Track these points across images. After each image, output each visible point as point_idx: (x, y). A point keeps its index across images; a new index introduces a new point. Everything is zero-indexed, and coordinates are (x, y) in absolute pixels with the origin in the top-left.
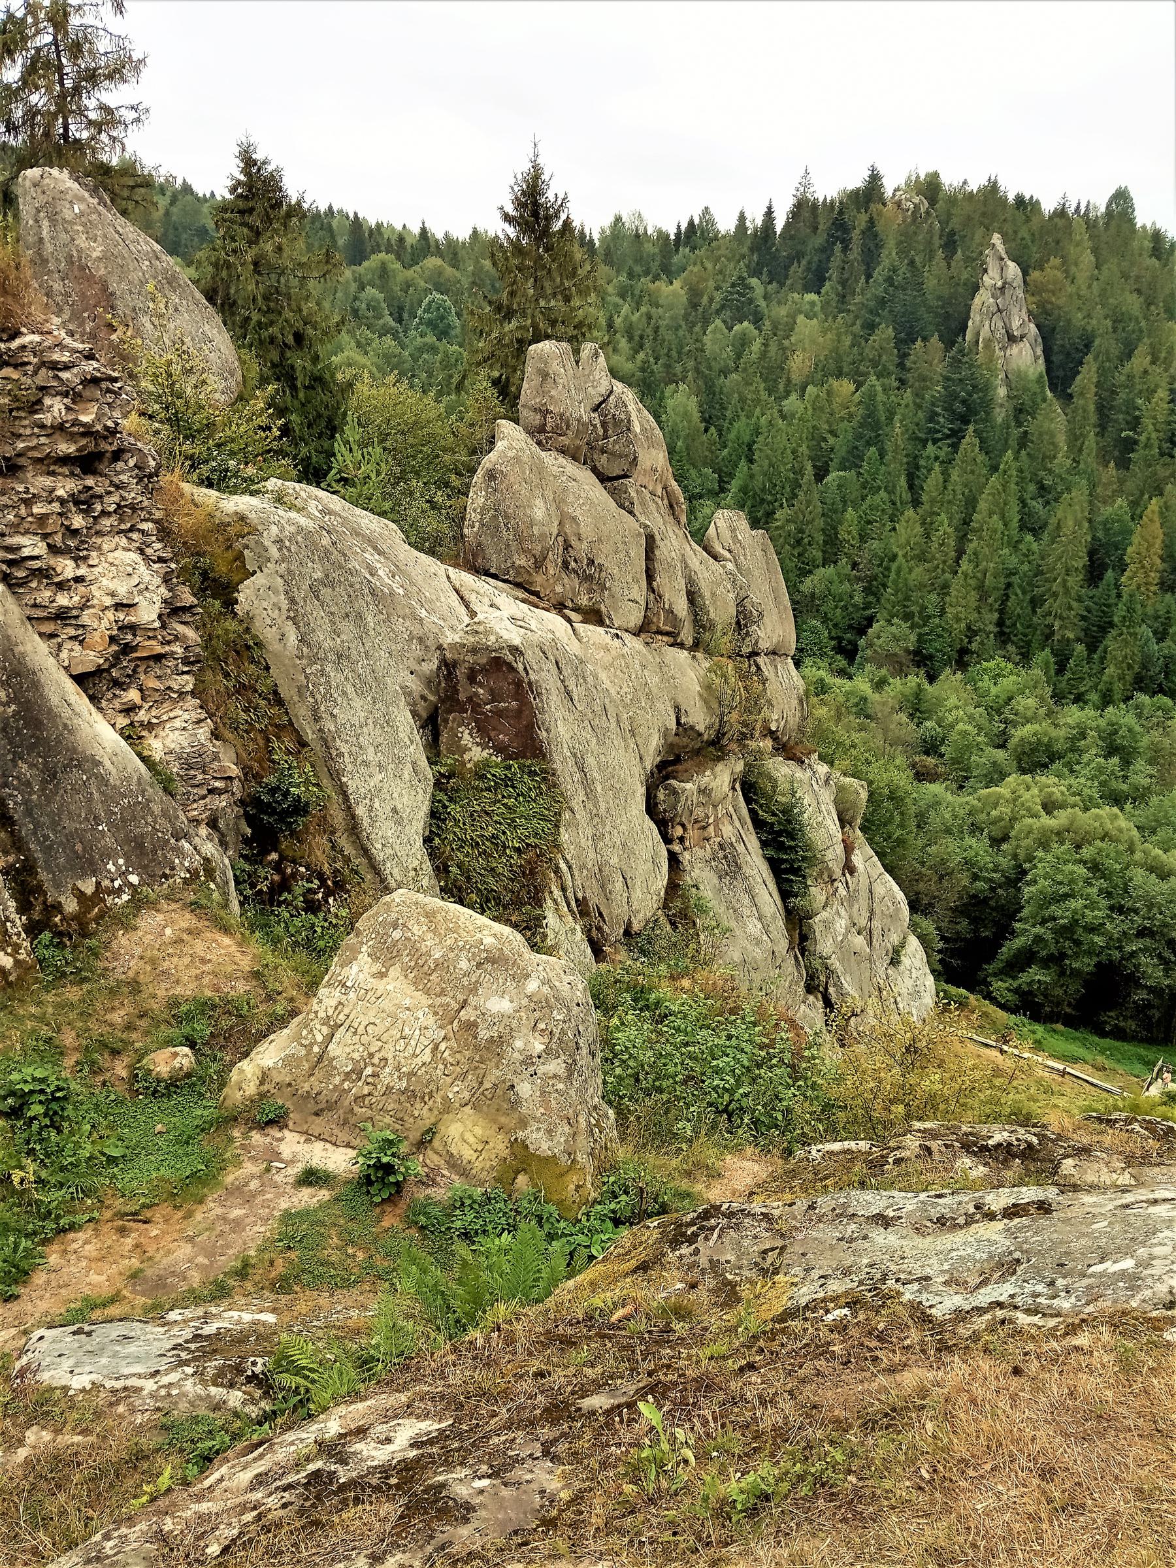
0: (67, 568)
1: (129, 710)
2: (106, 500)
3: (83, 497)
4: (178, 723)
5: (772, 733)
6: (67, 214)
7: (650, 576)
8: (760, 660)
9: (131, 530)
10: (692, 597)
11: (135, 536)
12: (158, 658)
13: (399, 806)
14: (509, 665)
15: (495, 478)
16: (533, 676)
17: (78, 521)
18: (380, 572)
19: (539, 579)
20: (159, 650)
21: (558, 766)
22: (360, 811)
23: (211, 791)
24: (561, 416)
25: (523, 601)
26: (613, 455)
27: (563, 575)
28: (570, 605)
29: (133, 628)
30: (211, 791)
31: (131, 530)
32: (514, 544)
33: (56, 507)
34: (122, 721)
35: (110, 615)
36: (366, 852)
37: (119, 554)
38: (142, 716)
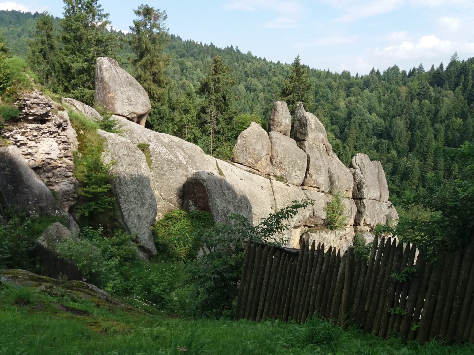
0: (33, 143)
1: (48, 178)
2: (45, 129)
3: (37, 129)
4: (64, 183)
5: (368, 225)
6: (103, 68)
7: (308, 169)
8: (364, 201)
9: (55, 137)
10: (330, 177)
11: (55, 138)
12: (60, 167)
13: (141, 214)
14: (202, 184)
15: (244, 137)
16: (209, 188)
17: (35, 134)
18: (180, 158)
19: (258, 166)
20: (60, 165)
21: (214, 214)
22: (125, 213)
23: (69, 200)
24: (279, 122)
25: (249, 171)
26: (302, 134)
27: (271, 166)
28: (273, 174)
29: (51, 159)
30: (69, 200)
31: (55, 137)
32: (248, 155)
33: (29, 130)
34: (46, 180)
35: (43, 155)
36: (126, 224)
37: (50, 142)
38: (52, 180)
